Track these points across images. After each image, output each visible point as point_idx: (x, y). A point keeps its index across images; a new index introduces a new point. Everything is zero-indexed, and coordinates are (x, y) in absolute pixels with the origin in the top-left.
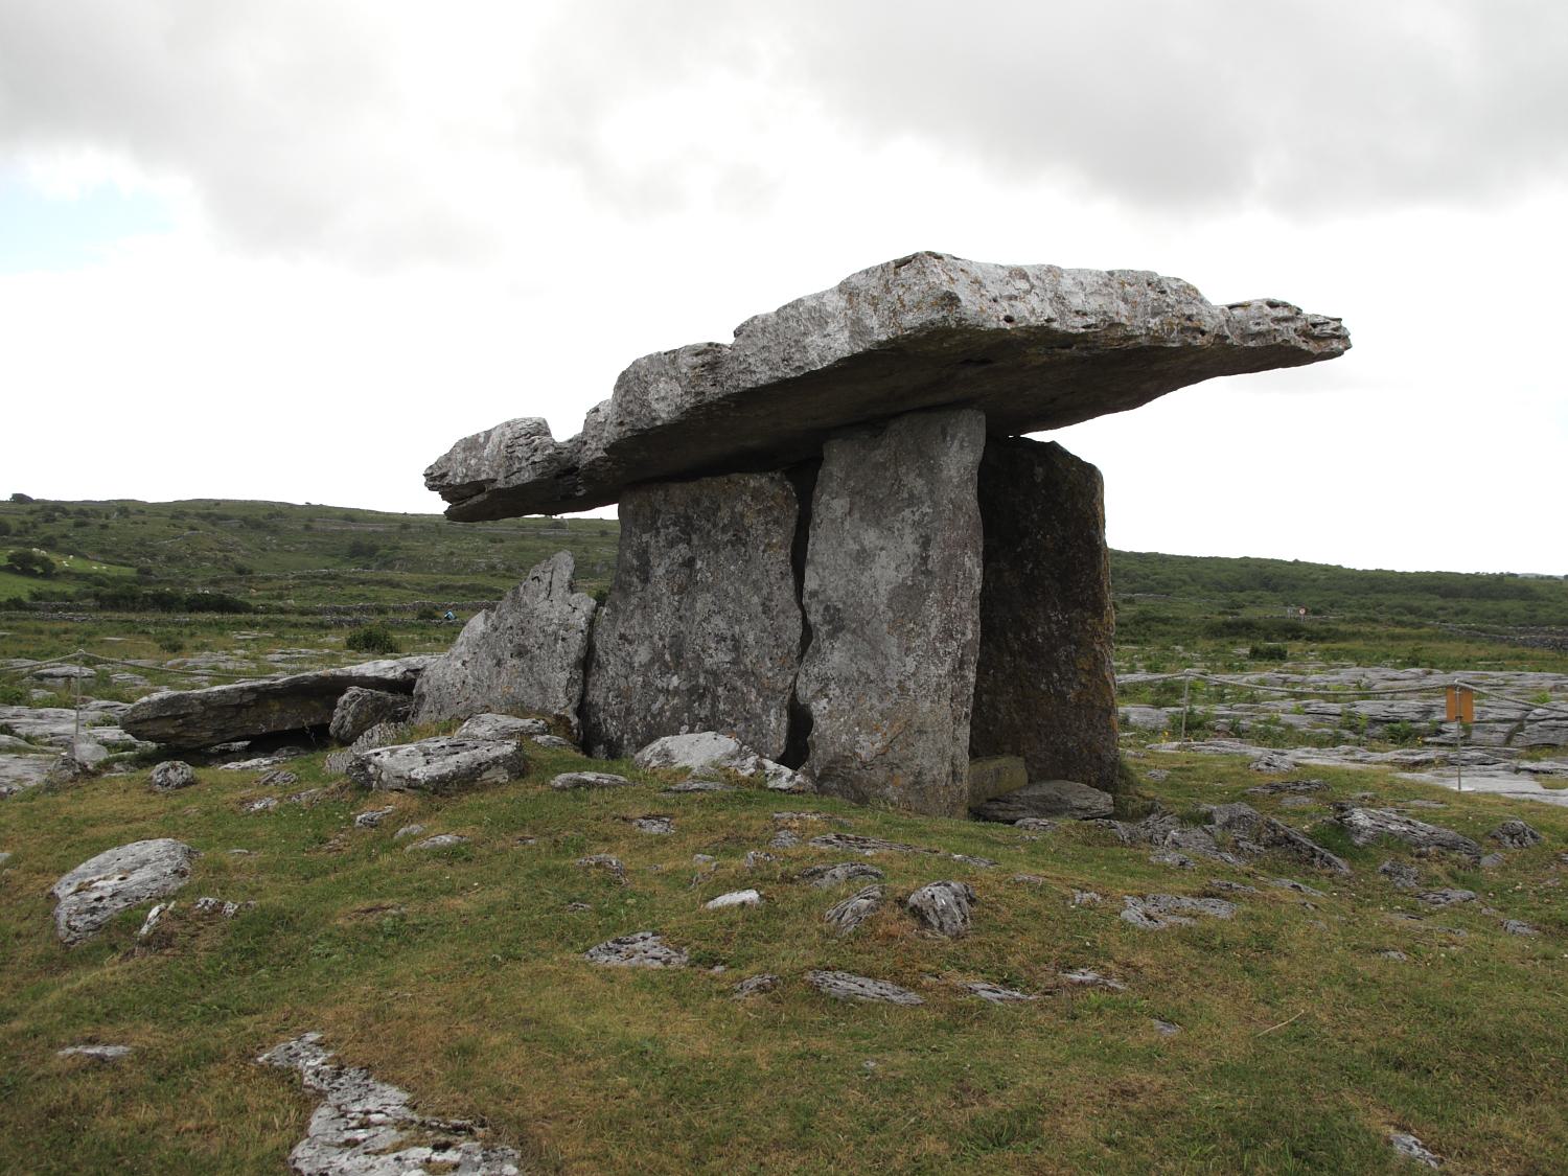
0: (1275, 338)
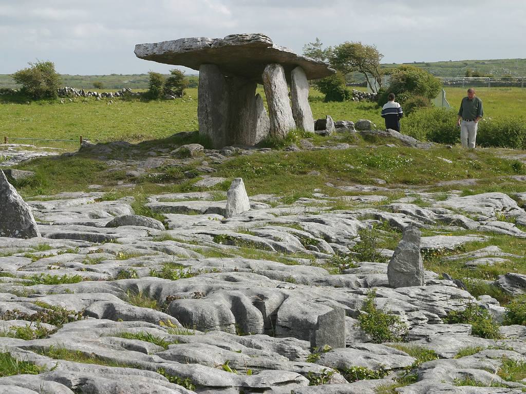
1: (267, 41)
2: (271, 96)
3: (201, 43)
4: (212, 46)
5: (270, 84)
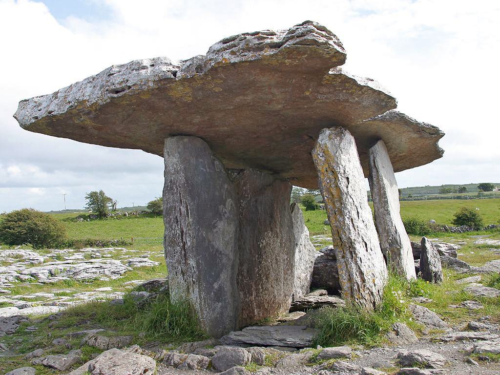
1: (331, 42)
2: (338, 205)
3: (150, 69)
4: (178, 74)
5: (335, 173)
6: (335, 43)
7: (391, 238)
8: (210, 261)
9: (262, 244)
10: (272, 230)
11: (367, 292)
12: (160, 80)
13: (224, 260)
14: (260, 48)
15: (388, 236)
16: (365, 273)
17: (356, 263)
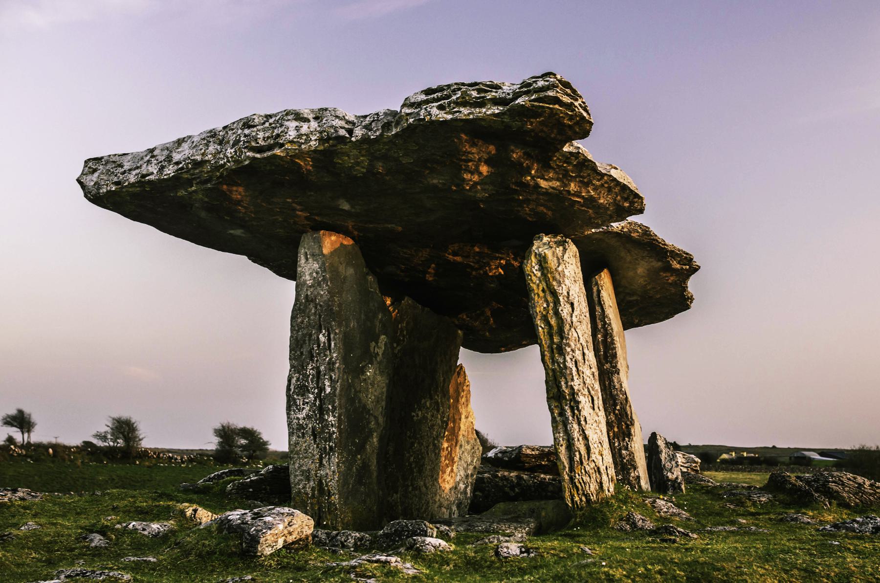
0: (407, 120)
1: (576, 104)
4: (359, 132)
5: (555, 294)
6: (580, 105)
7: (618, 407)
8: (356, 422)
9: (418, 415)
10: (431, 399)
11: (592, 465)
12: (329, 138)
13: (372, 425)
14: (481, 103)
15: (615, 405)
16: (590, 439)
17: (579, 424)
